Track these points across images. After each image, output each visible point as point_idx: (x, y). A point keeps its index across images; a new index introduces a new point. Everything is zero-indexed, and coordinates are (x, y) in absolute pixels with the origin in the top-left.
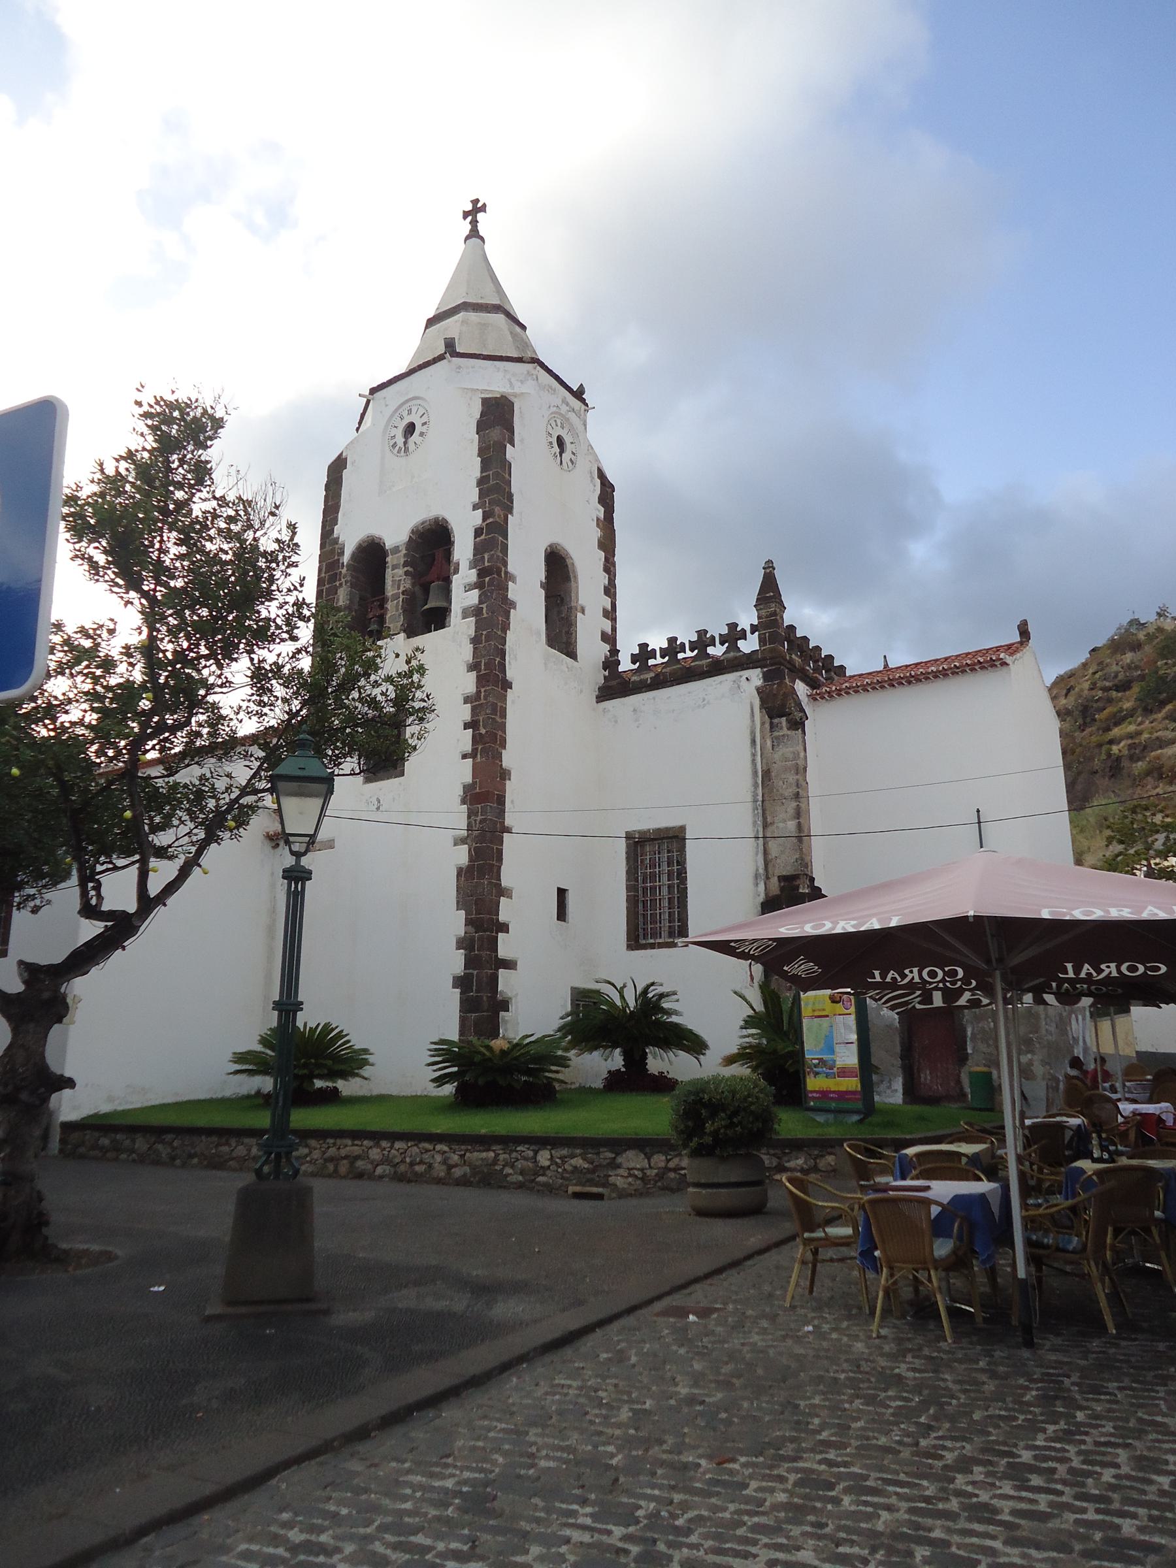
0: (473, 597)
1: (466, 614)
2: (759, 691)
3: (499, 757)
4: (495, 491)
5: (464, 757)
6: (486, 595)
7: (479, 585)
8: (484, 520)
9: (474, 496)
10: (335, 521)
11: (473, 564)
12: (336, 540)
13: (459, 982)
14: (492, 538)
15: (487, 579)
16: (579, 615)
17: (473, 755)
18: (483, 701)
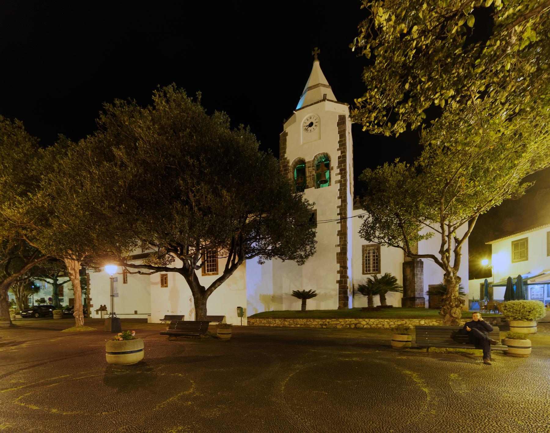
1: (336, 182)
13: (338, 282)
17: (341, 222)
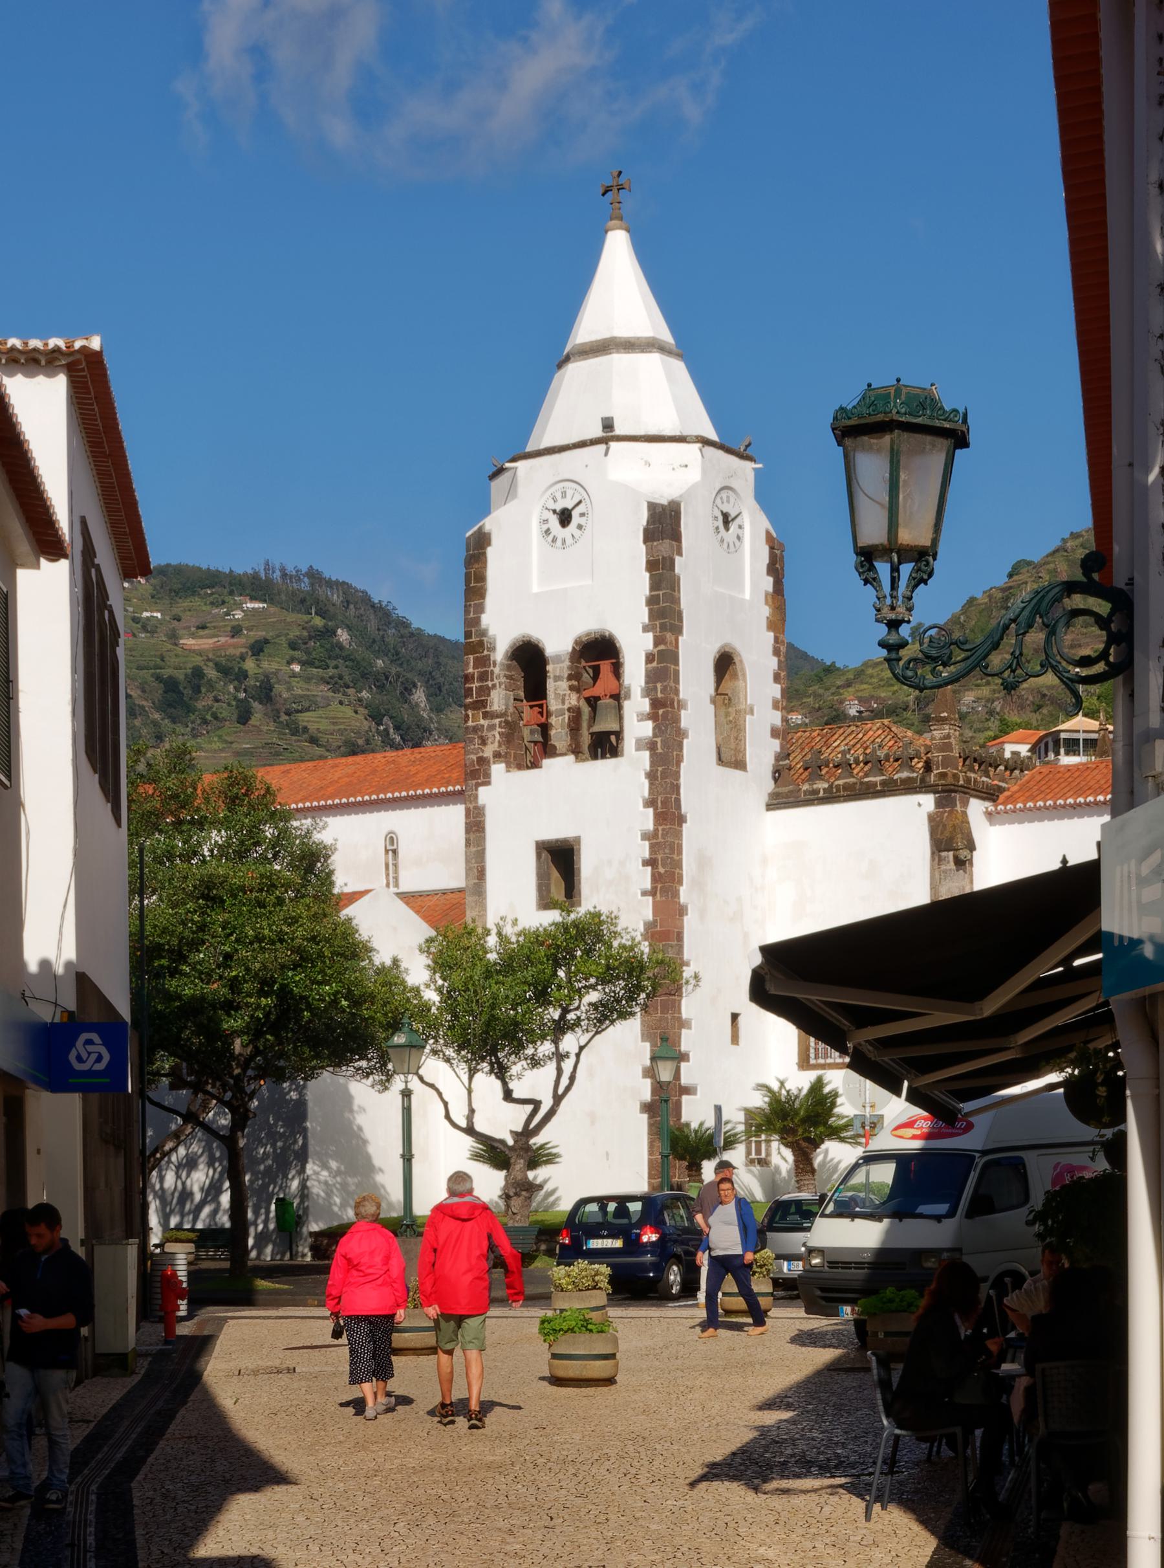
0: (647, 729)
1: (640, 745)
2: (931, 818)
3: (676, 894)
4: (665, 613)
5: (644, 893)
6: (660, 729)
7: (653, 716)
8: (656, 644)
9: (644, 615)
10: (480, 609)
11: (648, 691)
12: (484, 633)
14: (663, 666)
15: (661, 712)
16: (748, 717)
17: (653, 893)
18: (660, 840)
